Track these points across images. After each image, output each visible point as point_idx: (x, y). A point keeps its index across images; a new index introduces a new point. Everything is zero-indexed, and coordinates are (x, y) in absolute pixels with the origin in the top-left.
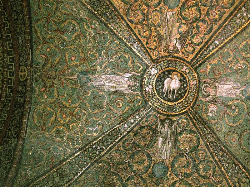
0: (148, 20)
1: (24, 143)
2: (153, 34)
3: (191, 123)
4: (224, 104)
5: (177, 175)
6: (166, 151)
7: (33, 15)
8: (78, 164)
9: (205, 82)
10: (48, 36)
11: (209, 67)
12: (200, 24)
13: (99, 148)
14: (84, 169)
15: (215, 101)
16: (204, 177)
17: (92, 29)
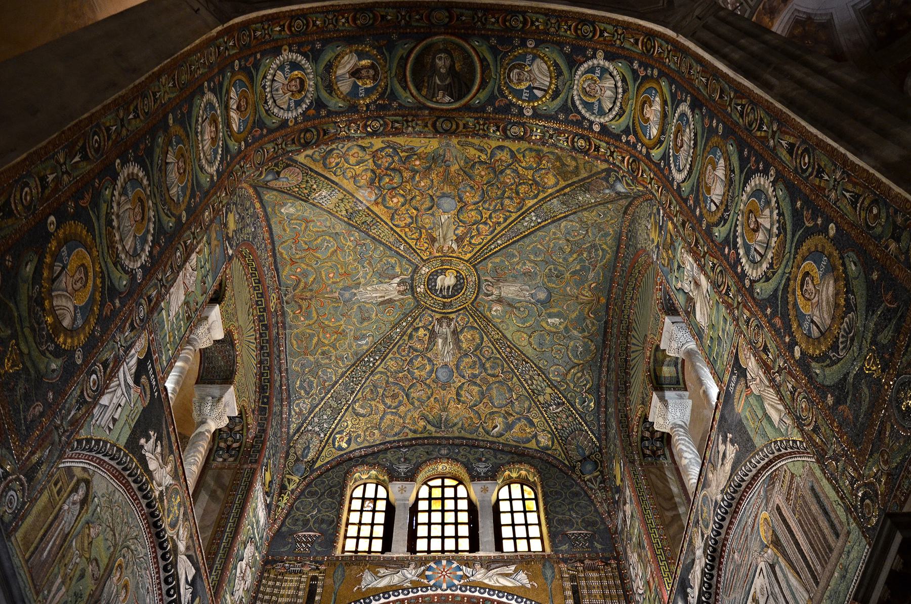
0: (416, 222)
1: (287, 373)
2: (423, 236)
3: (471, 320)
4: (510, 304)
5: (463, 377)
6: (448, 352)
7: (276, 239)
9: (486, 280)
10: (298, 256)
11: (490, 265)
12: (481, 226)
13: (372, 359)
15: (500, 300)
16: (493, 376)
17: (351, 241)
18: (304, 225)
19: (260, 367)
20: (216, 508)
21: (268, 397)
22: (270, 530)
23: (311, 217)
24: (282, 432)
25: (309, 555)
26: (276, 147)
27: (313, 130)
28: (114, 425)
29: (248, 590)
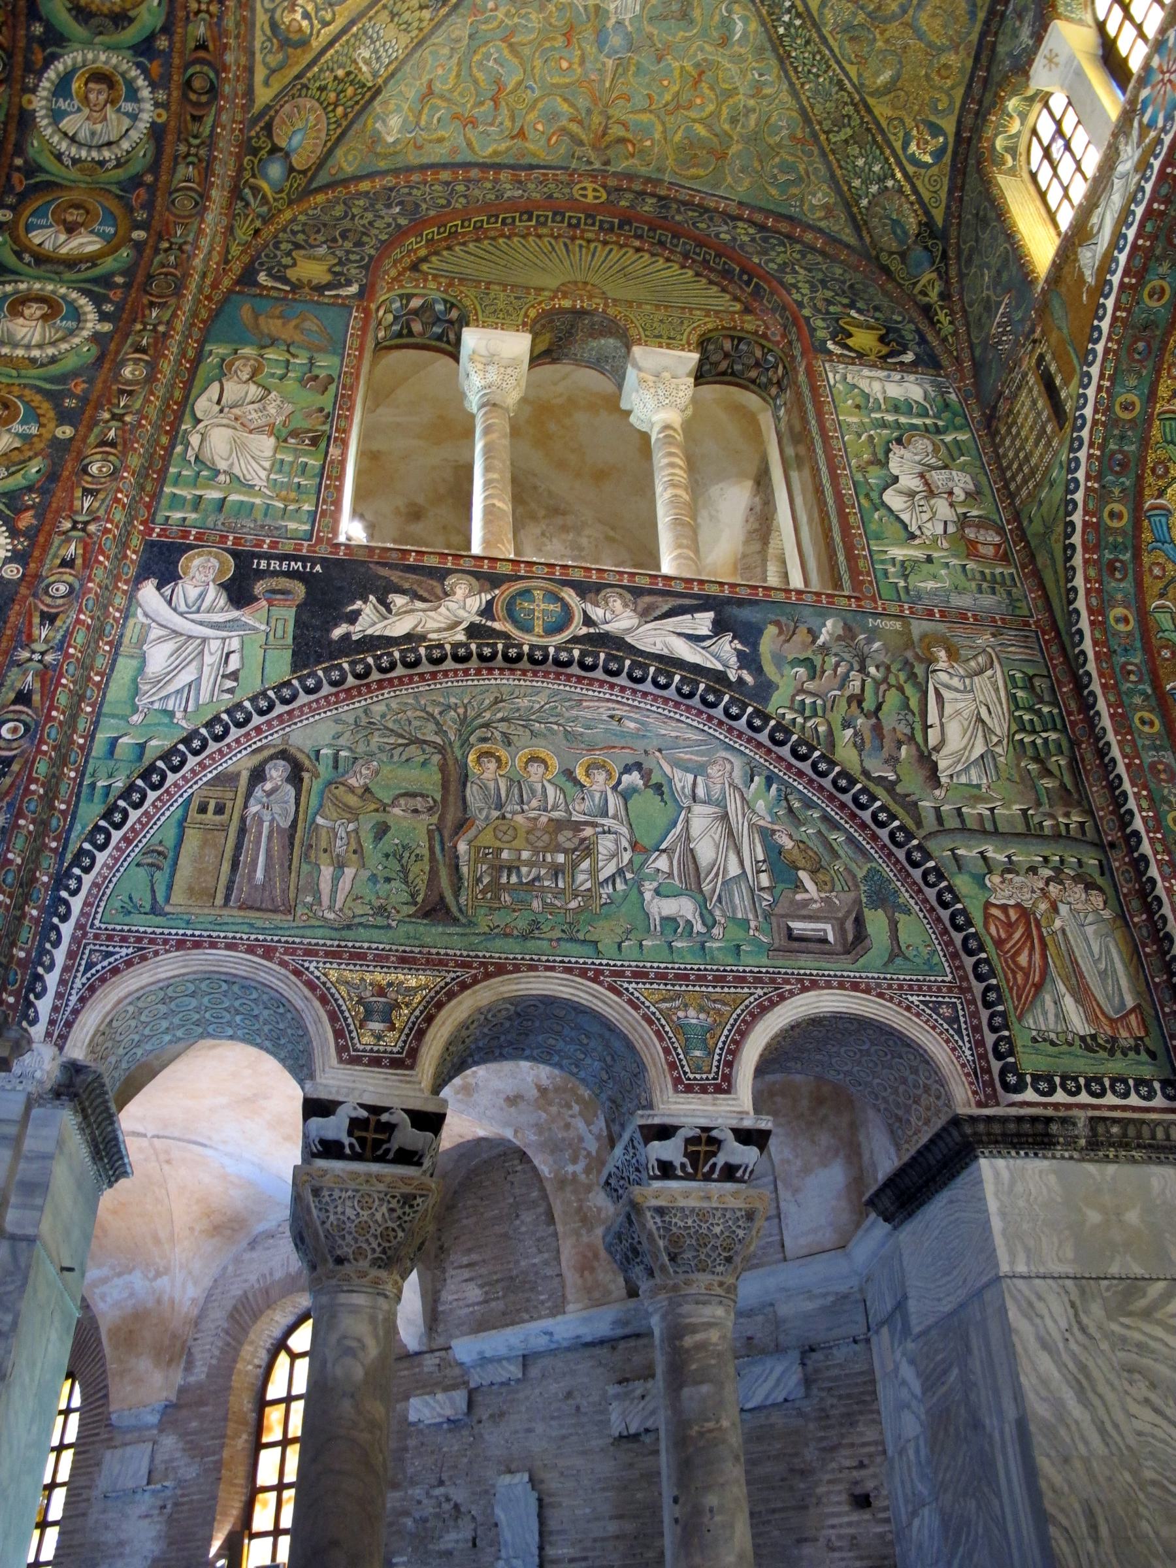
7: (459, 159)
8: (818, 76)
10: (508, 123)
13: (786, 18)
14: (832, 62)
17: (496, 9)
18: (439, 102)
19: (694, 261)
20: (807, 472)
21: (743, 271)
22: (962, 380)
23: (420, 84)
24: (842, 262)
25: (1017, 342)
26: (190, 159)
27: (190, 71)
28: (236, 680)
29: (973, 496)
